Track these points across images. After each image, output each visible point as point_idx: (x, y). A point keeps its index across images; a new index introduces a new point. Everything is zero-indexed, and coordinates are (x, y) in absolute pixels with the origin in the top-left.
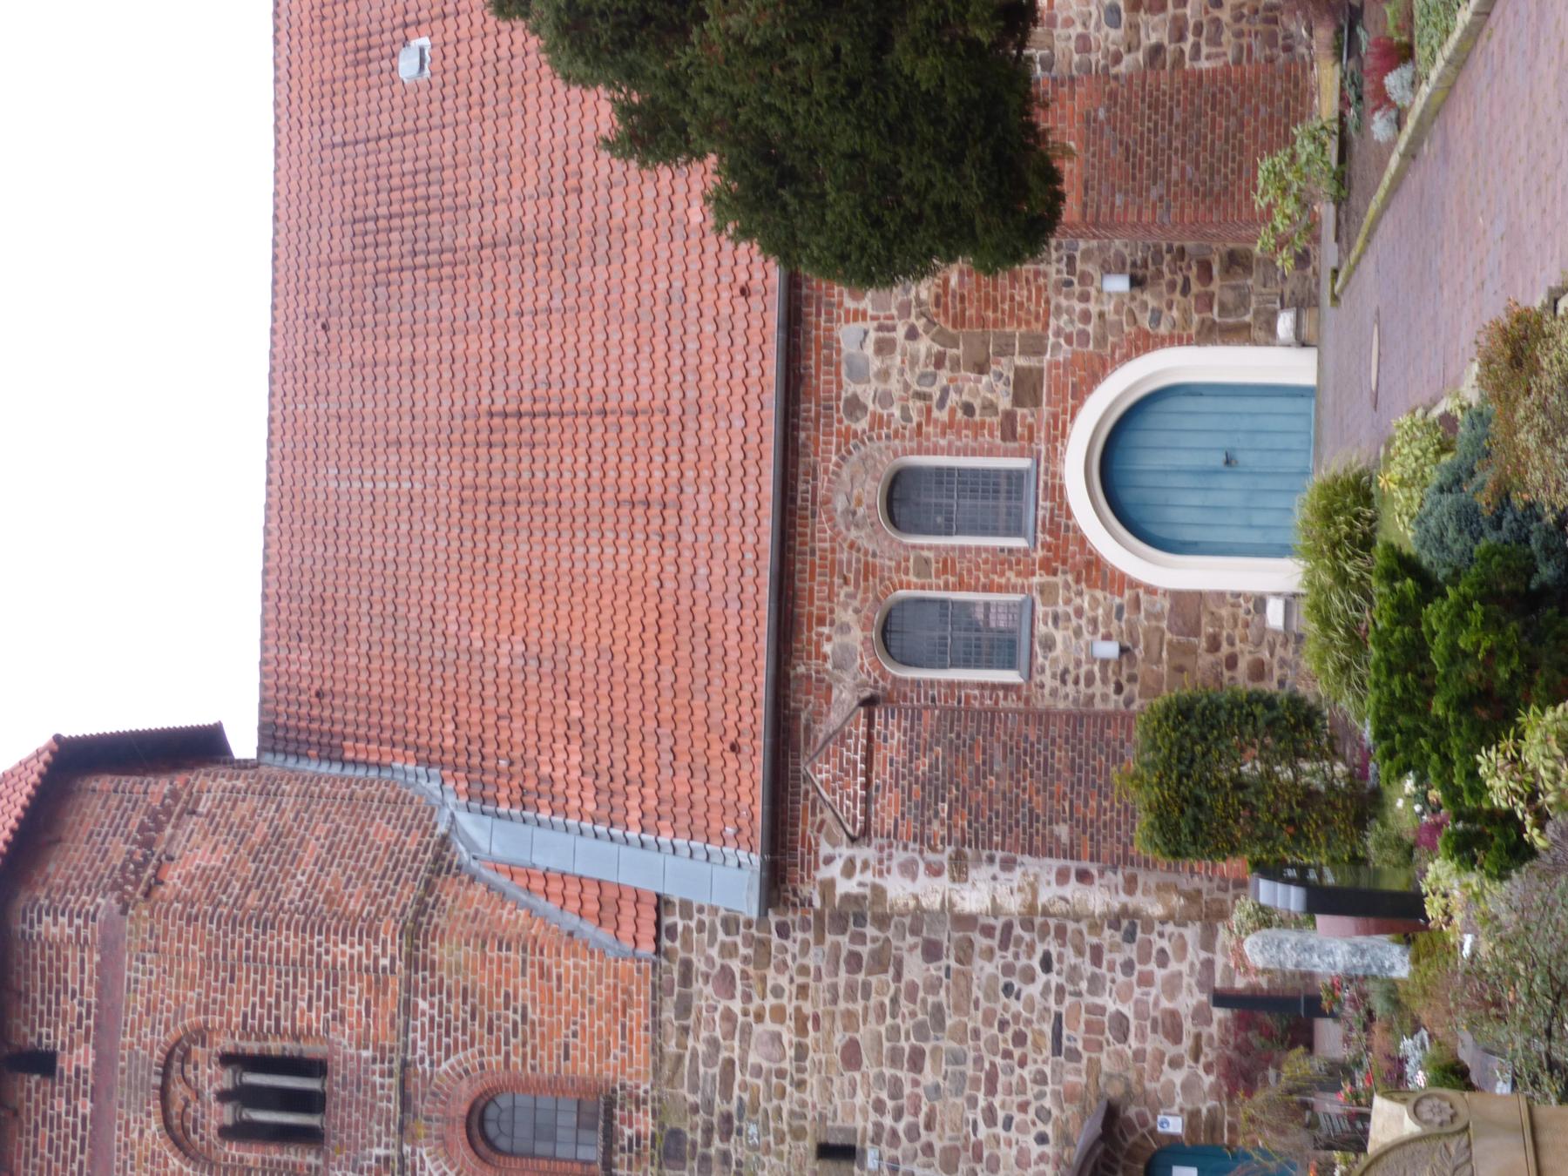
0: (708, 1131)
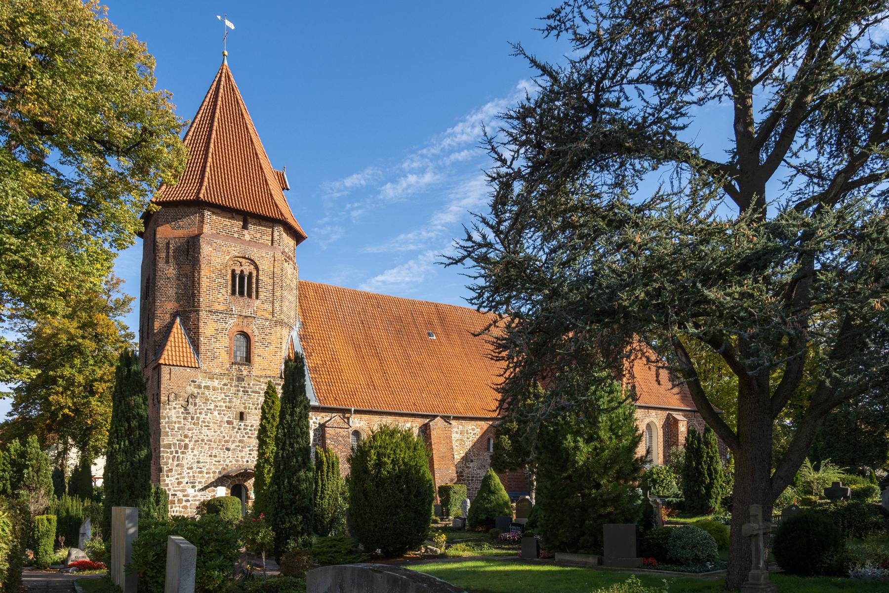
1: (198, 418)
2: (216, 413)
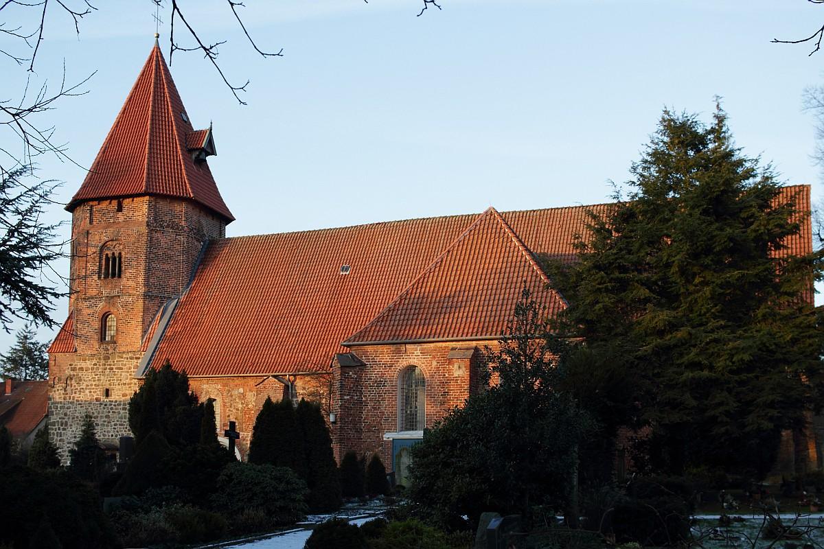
0: (110, 365)
1: (74, 397)
2: (87, 391)
